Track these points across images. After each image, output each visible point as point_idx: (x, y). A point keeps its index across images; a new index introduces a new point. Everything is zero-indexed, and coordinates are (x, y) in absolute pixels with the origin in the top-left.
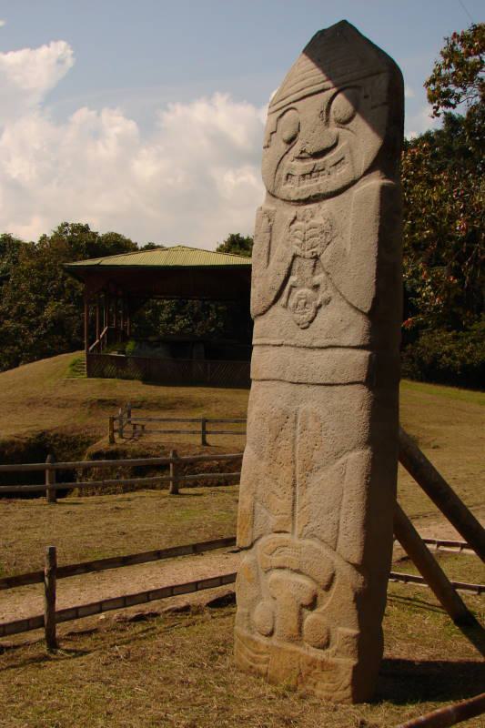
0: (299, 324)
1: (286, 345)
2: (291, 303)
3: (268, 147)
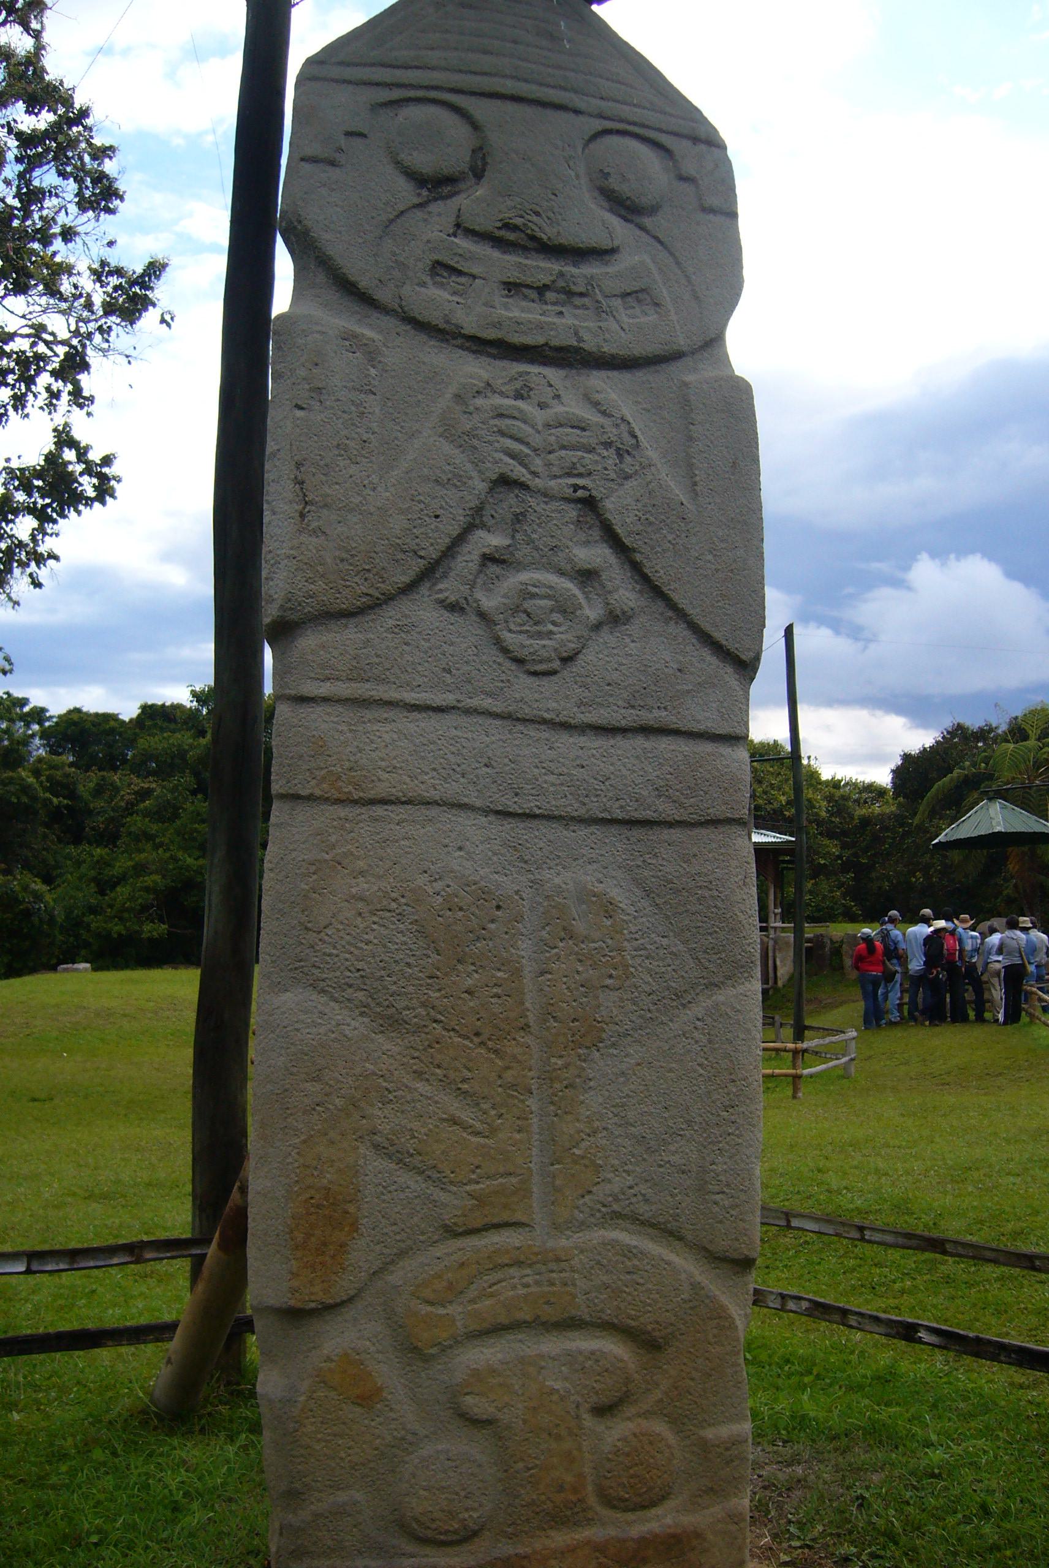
0: (519, 661)
1: (469, 711)
3: (332, 163)
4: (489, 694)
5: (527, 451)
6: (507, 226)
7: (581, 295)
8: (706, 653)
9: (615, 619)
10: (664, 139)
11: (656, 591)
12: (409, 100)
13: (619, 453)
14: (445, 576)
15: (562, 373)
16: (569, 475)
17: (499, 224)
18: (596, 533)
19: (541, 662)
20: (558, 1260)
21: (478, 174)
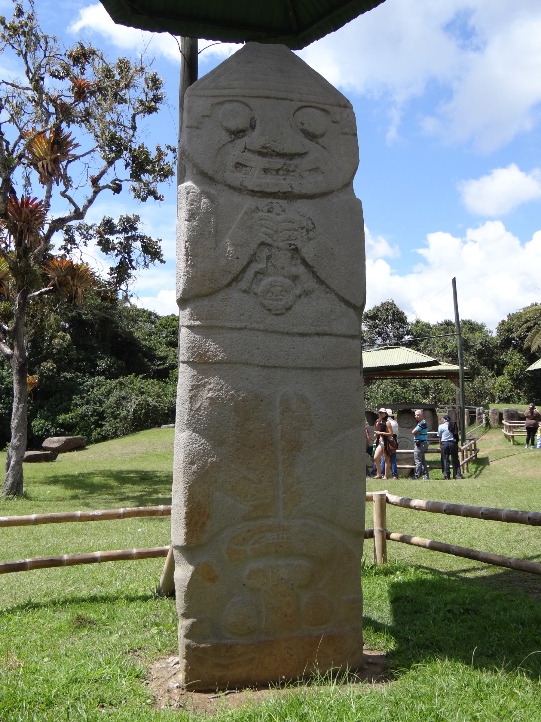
0: (269, 310)
1: (250, 329)
2: (259, 289)
3: (198, 128)
4: (258, 323)
5: (271, 232)
6: (263, 147)
7: (293, 171)
8: (342, 304)
9: (307, 293)
10: (327, 107)
11: (321, 282)
12: (226, 101)
13: (308, 231)
14: (241, 280)
15: (286, 201)
16: (288, 240)
17: (260, 147)
18: (299, 262)
19: (278, 310)
20: (284, 530)
21: (253, 127)
